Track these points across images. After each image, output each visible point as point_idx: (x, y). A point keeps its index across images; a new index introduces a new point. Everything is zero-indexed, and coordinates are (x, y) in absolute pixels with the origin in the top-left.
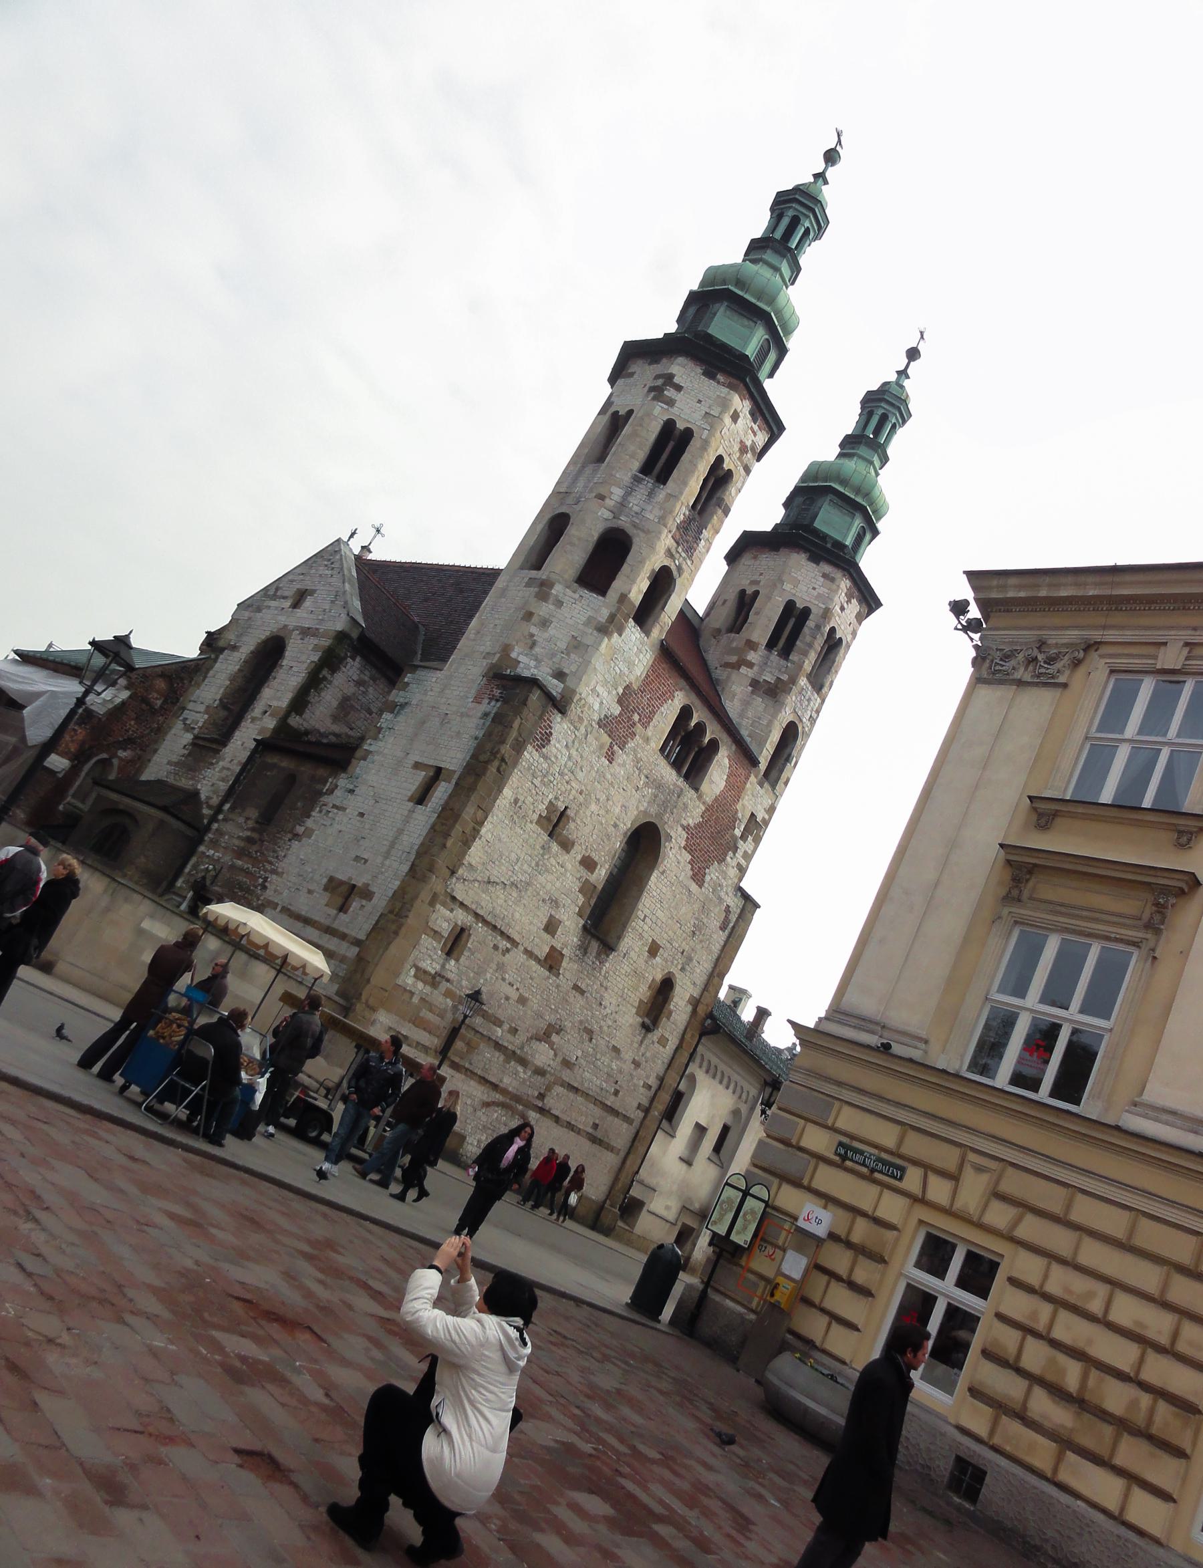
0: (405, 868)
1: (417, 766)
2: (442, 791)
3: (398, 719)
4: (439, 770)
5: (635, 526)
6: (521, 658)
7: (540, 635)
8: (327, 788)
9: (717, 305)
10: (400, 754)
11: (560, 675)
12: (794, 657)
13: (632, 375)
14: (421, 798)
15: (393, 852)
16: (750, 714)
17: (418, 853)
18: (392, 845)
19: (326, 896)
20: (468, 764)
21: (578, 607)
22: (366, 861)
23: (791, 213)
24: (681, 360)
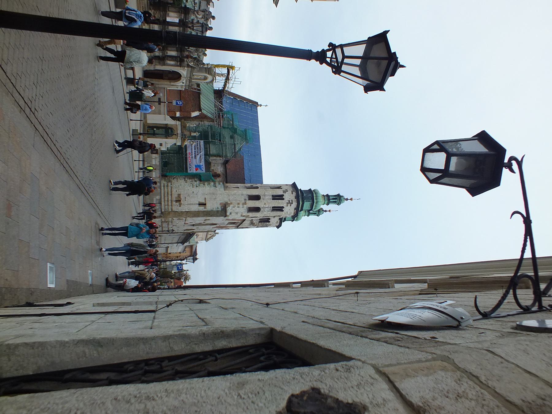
0: (187, 211)
1: (205, 199)
2: (202, 208)
3: (213, 187)
4: (205, 204)
5: (262, 211)
6: (231, 207)
7: (236, 208)
8: (195, 179)
9: (311, 201)
10: (206, 194)
11: (231, 214)
12: (260, 224)
13: (292, 194)
14: (200, 204)
15: (189, 205)
16: (246, 222)
17: (190, 211)
18: (190, 204)
19: (177, 196)
20: (208, 211)
21: (244, 210)
22: (185, 200)
23: (337, 201)
24: (296, 203)
